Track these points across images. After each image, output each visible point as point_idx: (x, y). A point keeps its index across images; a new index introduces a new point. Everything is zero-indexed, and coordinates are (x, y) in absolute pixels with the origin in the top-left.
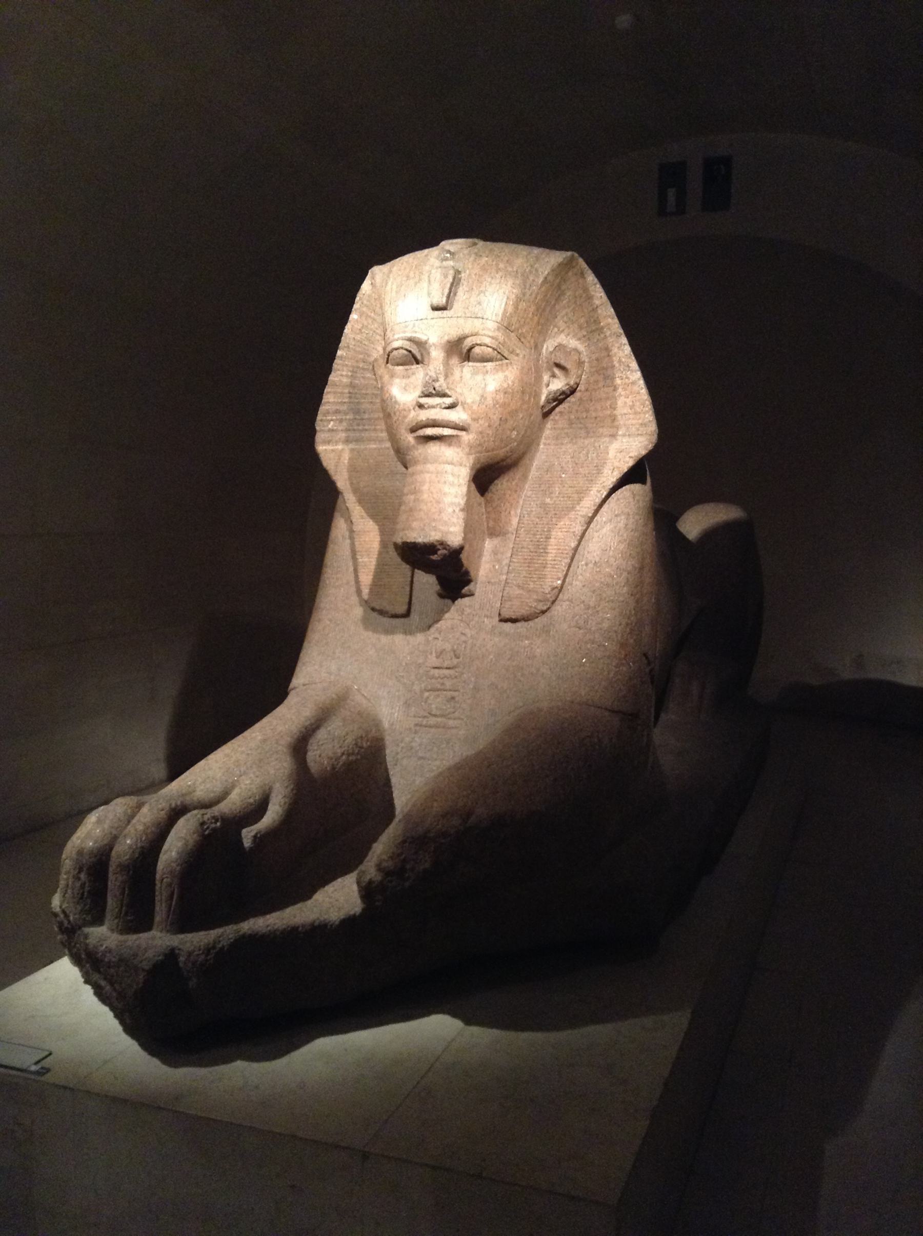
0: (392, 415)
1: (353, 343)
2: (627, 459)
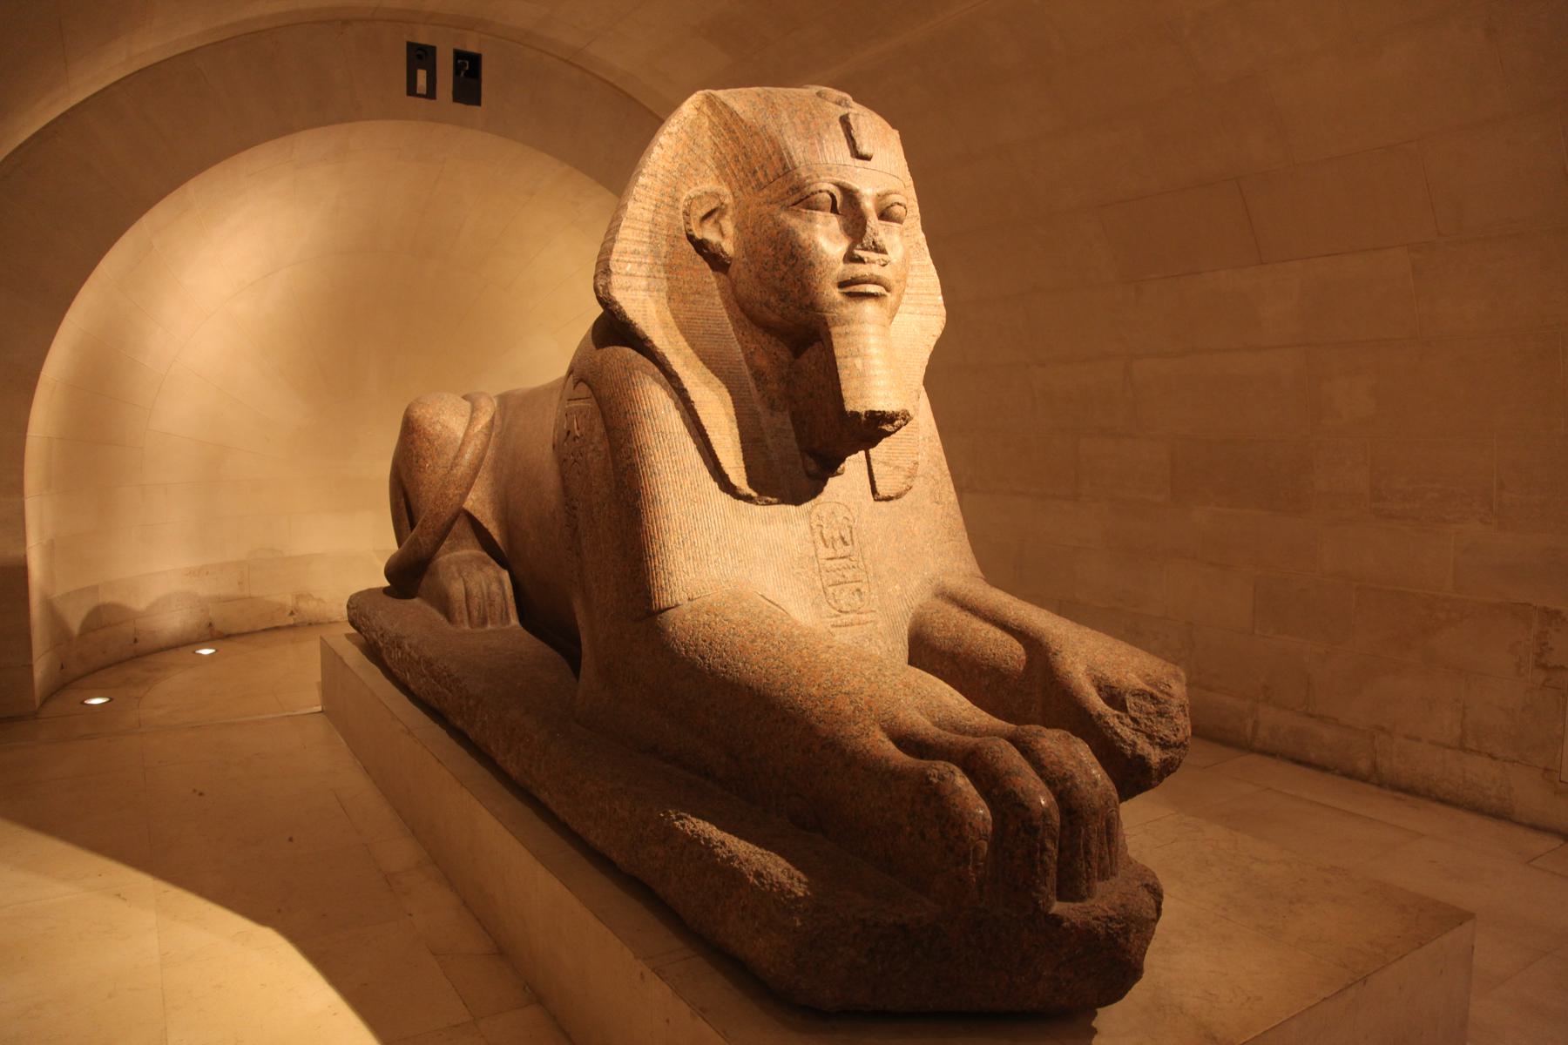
0: (817, 265)
1: (662, 172)
2: (932, 338)
